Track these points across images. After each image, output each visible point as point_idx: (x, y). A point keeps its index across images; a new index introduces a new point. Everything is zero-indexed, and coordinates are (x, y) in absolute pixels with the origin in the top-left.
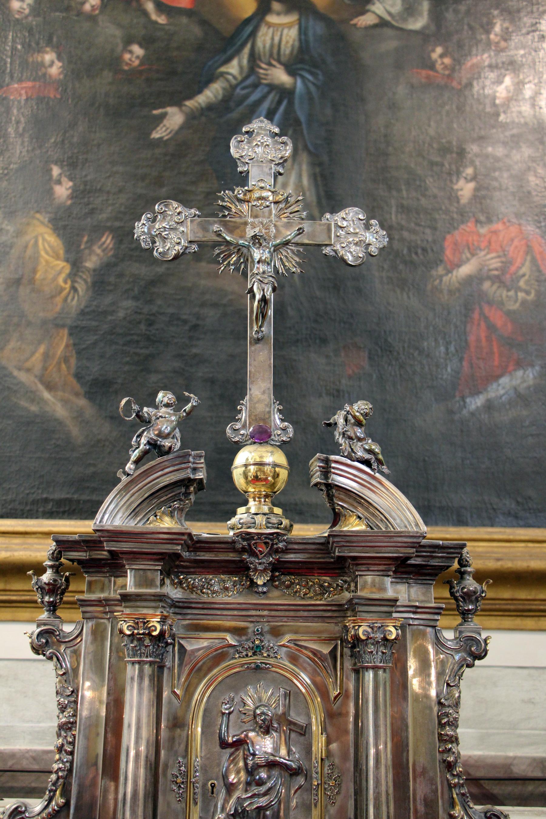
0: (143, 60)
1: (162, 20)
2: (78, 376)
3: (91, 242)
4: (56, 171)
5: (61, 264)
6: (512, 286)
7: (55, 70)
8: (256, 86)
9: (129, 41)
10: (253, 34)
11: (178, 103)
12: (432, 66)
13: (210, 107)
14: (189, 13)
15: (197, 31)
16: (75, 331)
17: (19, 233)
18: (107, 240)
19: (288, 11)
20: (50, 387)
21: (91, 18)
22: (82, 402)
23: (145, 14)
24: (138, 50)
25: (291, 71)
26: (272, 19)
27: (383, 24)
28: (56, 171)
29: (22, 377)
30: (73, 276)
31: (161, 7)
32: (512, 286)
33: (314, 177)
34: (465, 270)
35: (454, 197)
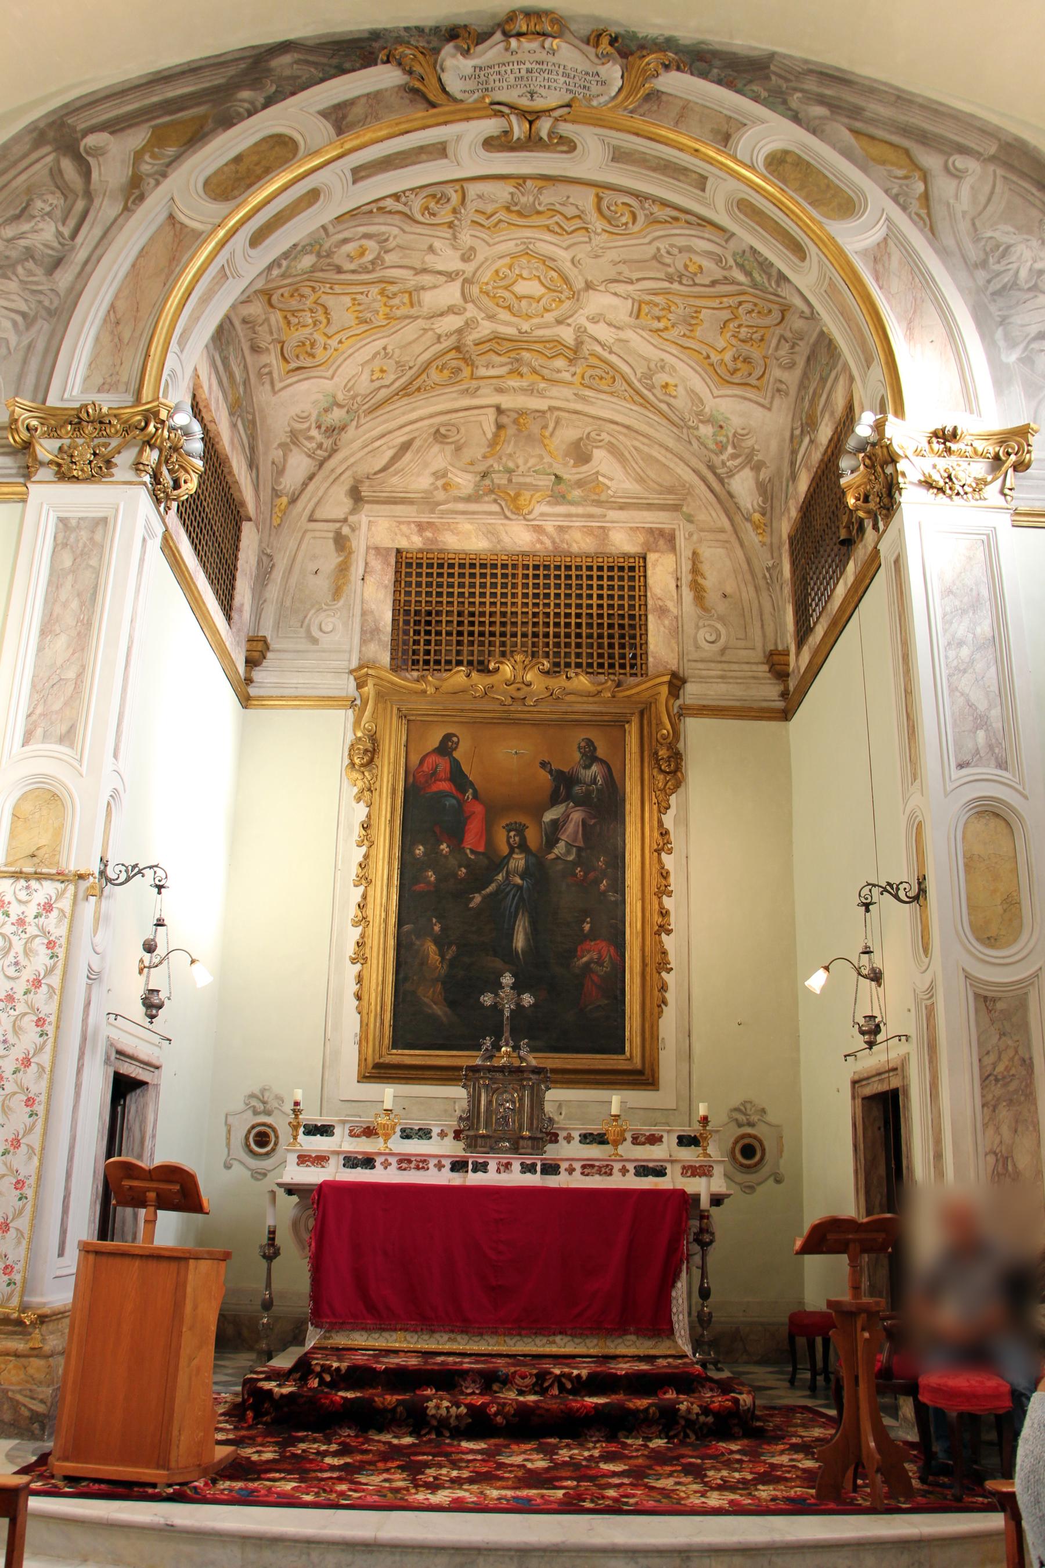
0: (466, 874)
1: (473, 857)
2: (445, 1000)
3: (448, 949)
4: (434, 920)
5: (437, 957)
6: (602, 965)
7: (432, 879)
8: (508, 885)
9: (460, 866)
10: (508, 863)
11: (479, 892)
12: (575, 875)
13: (491, 894)
14: (483, 854)
15: (486, 861)
16: (444, 983)
17: (422, 945)
18: (454, 948)
19: (521, 853)
20: (435, 1004)
21: (446, 857)
22: (447, 1009)
23: (466, 855)
24: (464, 870)
25: (522, 879)
26: (515, 856)
27: (558, 858)
28: (434, 920)
29: (426, 1000)
30: (441, 962)
31: (472, 851)
32: (602, 965)
33: (530, 922)
34: (585, 959)
35: (582, 930)
